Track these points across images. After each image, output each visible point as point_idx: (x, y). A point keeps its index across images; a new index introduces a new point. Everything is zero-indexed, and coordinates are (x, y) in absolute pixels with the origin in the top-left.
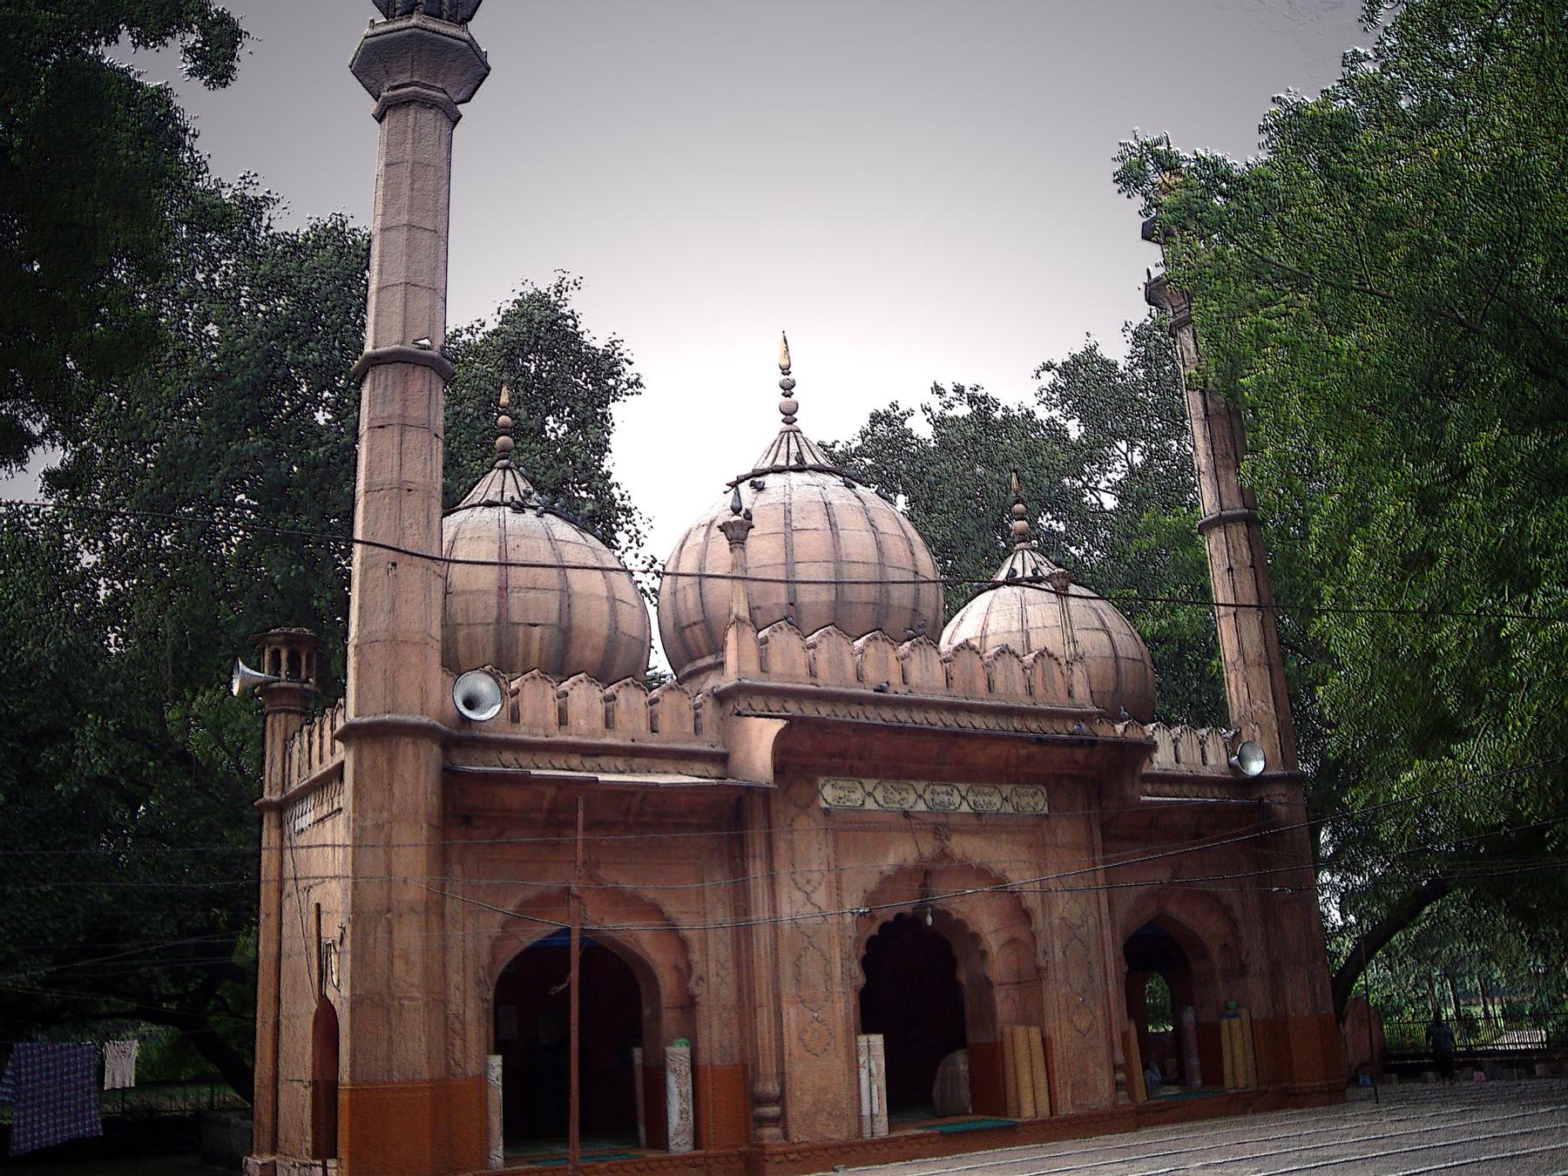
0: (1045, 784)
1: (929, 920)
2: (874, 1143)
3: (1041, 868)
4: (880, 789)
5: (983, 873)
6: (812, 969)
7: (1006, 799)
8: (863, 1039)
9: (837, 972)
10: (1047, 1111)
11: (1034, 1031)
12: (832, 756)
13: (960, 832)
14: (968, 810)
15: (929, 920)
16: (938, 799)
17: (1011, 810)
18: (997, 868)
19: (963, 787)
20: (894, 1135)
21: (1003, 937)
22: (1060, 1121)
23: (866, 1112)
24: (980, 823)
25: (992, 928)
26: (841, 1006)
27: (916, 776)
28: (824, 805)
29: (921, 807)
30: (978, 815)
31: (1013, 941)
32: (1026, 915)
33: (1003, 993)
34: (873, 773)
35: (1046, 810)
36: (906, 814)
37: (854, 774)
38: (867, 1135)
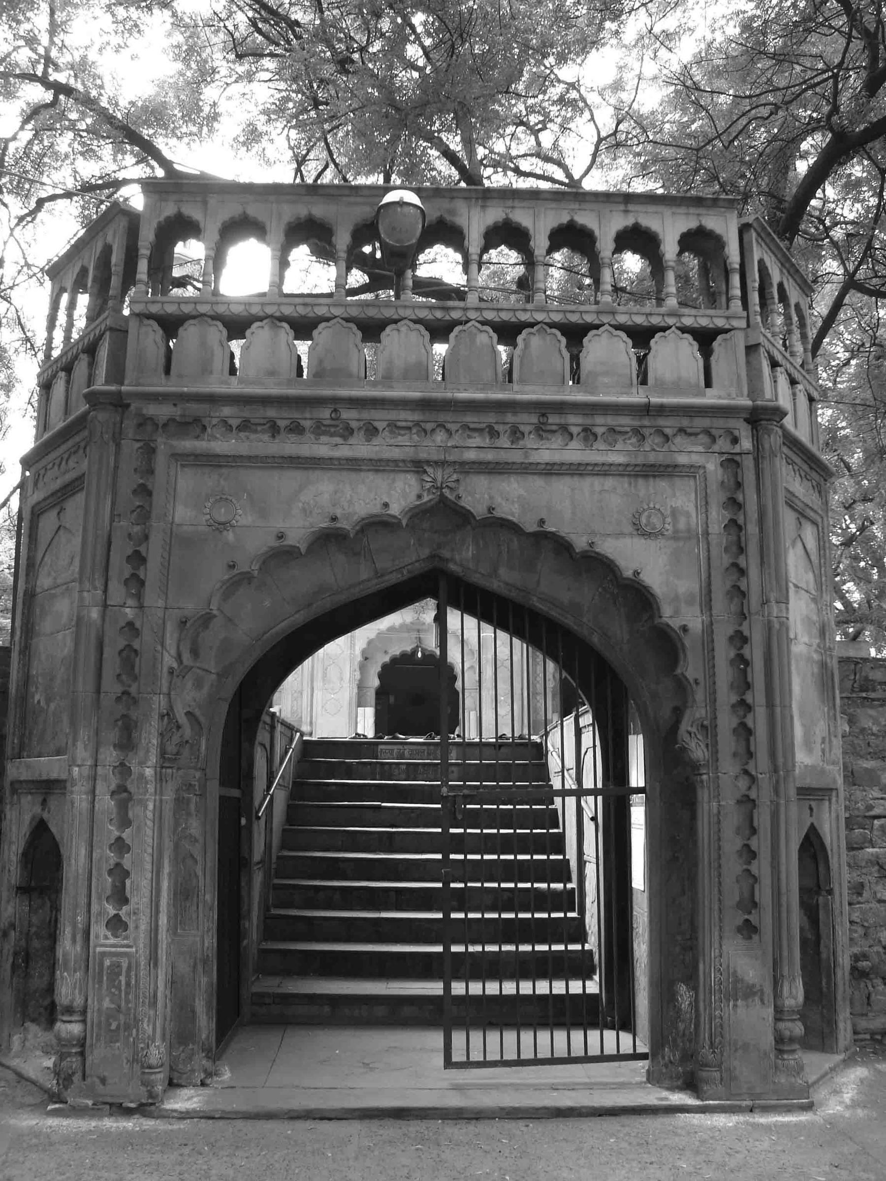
1: (420, 655)
6: (333, 673)
8: (360, 710)
9: (347, 675)
15: (420, 655)
26: (347, 693)
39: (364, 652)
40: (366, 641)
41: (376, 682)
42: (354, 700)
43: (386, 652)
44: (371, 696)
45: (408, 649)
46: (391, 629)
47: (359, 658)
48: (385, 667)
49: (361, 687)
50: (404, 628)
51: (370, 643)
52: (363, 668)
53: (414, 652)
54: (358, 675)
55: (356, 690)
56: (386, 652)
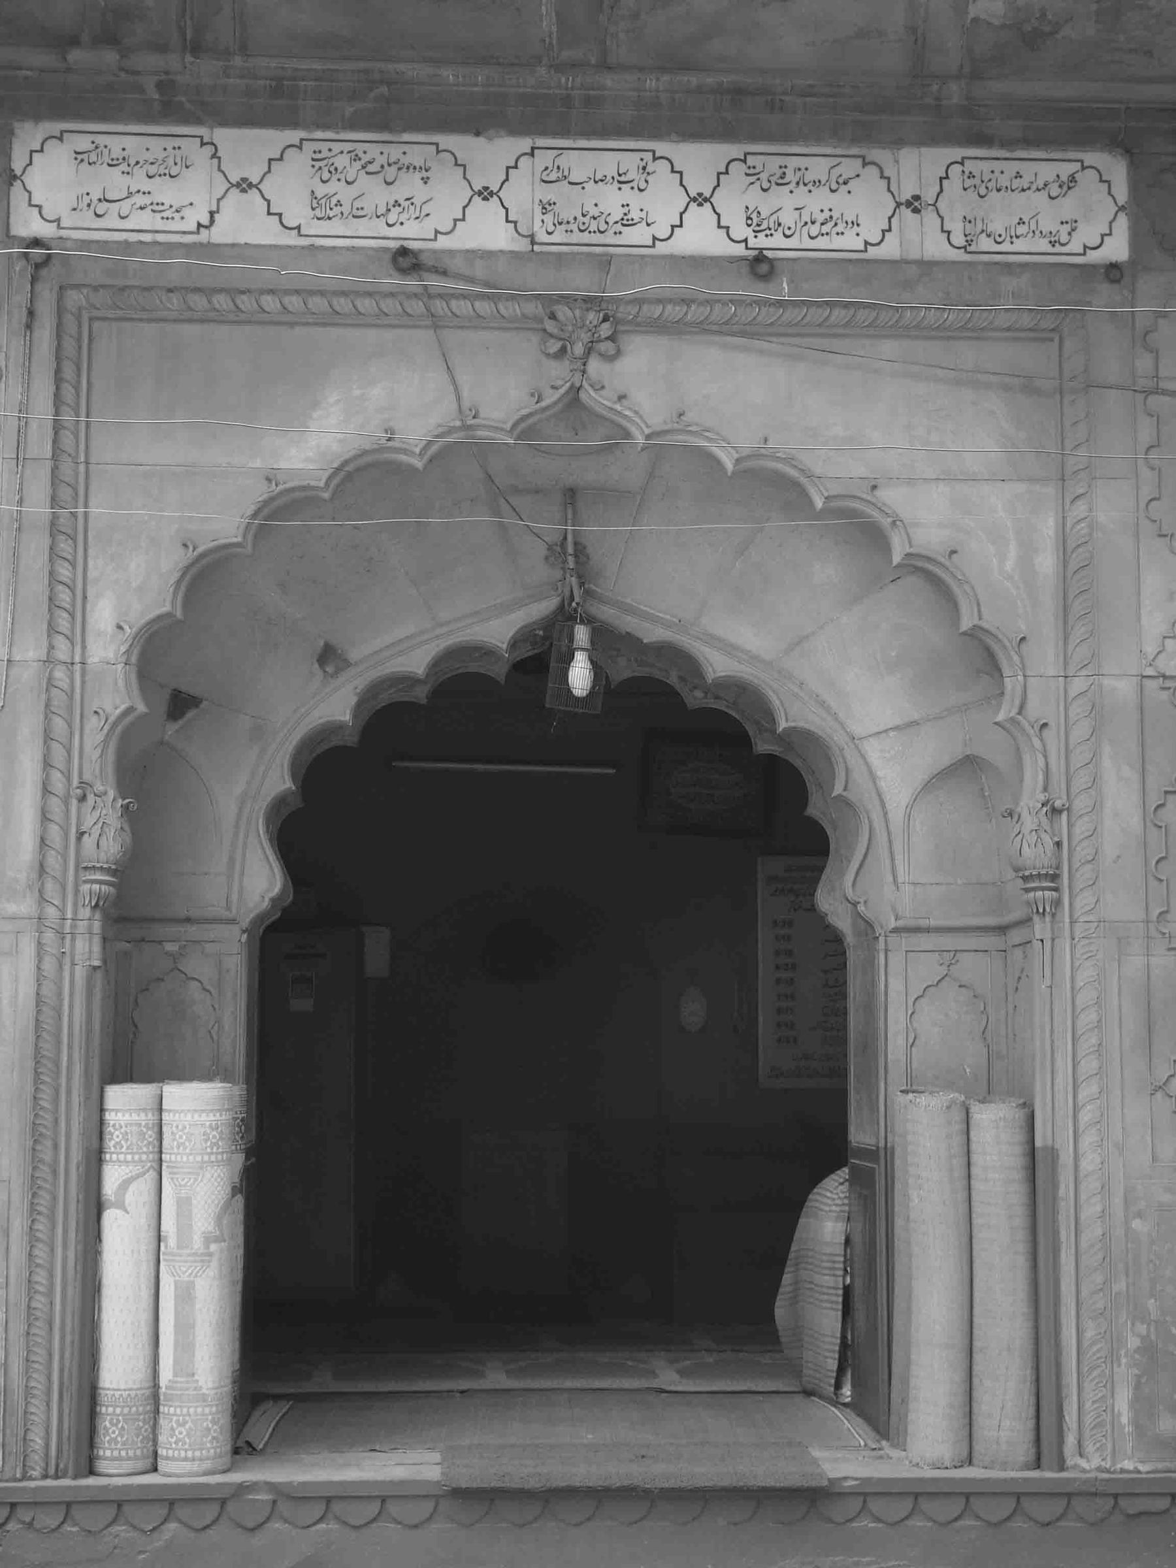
0: (1125, 145)
1: (580, 676)
2: (173, 1501)
3: (1064, 477)
4: (299, 162)
5: (772, 488)
7: (914, 204)
8: (125, 1103)
10: (1023, 1451)
11: (994, 1124)
12: (74, 42)
13: (659, 327)
14: (716, 245)
15: (580, 676)
16: (569, 203)
17: (936, 248)
18: (833, 468)
19: (699, 159)
20: (236, 1477)
21: (933, 751)
22: (1068, 1495)
23: (119, 1370)
24: (762, 299)
25: (890, 718)
27: (480, 118)
28: (27, 225)
29: (488, 231)
30: (760, 265)
31: (967, 768)
32: (983, 658)
33: (928, 969)
34: (275, 104)
35: (1117, 249)
36: (406, 260)
37: (173, 105)
38: (118, 1461)
39: (153, 649)
40: (172, 561)
41: (260, 881)
42: (78, 1013)
43: (329, 657)
44: (218, 986)
45: (498, 631)
46: (368, 476)
47: (114, 695)
48: (326, 768)
49: (135, 913)
50: (463, 462)
51: (206, 576)
52: (148, 772)
53: (540, 658)
54: (104, 833)
55: (87, 949)
56: (329, 657)
